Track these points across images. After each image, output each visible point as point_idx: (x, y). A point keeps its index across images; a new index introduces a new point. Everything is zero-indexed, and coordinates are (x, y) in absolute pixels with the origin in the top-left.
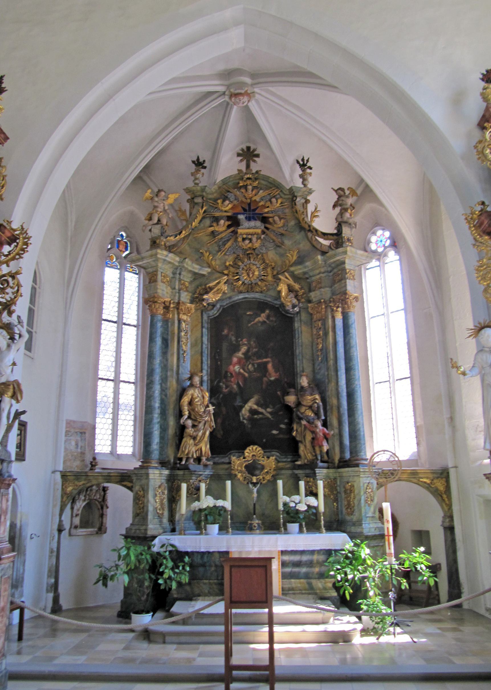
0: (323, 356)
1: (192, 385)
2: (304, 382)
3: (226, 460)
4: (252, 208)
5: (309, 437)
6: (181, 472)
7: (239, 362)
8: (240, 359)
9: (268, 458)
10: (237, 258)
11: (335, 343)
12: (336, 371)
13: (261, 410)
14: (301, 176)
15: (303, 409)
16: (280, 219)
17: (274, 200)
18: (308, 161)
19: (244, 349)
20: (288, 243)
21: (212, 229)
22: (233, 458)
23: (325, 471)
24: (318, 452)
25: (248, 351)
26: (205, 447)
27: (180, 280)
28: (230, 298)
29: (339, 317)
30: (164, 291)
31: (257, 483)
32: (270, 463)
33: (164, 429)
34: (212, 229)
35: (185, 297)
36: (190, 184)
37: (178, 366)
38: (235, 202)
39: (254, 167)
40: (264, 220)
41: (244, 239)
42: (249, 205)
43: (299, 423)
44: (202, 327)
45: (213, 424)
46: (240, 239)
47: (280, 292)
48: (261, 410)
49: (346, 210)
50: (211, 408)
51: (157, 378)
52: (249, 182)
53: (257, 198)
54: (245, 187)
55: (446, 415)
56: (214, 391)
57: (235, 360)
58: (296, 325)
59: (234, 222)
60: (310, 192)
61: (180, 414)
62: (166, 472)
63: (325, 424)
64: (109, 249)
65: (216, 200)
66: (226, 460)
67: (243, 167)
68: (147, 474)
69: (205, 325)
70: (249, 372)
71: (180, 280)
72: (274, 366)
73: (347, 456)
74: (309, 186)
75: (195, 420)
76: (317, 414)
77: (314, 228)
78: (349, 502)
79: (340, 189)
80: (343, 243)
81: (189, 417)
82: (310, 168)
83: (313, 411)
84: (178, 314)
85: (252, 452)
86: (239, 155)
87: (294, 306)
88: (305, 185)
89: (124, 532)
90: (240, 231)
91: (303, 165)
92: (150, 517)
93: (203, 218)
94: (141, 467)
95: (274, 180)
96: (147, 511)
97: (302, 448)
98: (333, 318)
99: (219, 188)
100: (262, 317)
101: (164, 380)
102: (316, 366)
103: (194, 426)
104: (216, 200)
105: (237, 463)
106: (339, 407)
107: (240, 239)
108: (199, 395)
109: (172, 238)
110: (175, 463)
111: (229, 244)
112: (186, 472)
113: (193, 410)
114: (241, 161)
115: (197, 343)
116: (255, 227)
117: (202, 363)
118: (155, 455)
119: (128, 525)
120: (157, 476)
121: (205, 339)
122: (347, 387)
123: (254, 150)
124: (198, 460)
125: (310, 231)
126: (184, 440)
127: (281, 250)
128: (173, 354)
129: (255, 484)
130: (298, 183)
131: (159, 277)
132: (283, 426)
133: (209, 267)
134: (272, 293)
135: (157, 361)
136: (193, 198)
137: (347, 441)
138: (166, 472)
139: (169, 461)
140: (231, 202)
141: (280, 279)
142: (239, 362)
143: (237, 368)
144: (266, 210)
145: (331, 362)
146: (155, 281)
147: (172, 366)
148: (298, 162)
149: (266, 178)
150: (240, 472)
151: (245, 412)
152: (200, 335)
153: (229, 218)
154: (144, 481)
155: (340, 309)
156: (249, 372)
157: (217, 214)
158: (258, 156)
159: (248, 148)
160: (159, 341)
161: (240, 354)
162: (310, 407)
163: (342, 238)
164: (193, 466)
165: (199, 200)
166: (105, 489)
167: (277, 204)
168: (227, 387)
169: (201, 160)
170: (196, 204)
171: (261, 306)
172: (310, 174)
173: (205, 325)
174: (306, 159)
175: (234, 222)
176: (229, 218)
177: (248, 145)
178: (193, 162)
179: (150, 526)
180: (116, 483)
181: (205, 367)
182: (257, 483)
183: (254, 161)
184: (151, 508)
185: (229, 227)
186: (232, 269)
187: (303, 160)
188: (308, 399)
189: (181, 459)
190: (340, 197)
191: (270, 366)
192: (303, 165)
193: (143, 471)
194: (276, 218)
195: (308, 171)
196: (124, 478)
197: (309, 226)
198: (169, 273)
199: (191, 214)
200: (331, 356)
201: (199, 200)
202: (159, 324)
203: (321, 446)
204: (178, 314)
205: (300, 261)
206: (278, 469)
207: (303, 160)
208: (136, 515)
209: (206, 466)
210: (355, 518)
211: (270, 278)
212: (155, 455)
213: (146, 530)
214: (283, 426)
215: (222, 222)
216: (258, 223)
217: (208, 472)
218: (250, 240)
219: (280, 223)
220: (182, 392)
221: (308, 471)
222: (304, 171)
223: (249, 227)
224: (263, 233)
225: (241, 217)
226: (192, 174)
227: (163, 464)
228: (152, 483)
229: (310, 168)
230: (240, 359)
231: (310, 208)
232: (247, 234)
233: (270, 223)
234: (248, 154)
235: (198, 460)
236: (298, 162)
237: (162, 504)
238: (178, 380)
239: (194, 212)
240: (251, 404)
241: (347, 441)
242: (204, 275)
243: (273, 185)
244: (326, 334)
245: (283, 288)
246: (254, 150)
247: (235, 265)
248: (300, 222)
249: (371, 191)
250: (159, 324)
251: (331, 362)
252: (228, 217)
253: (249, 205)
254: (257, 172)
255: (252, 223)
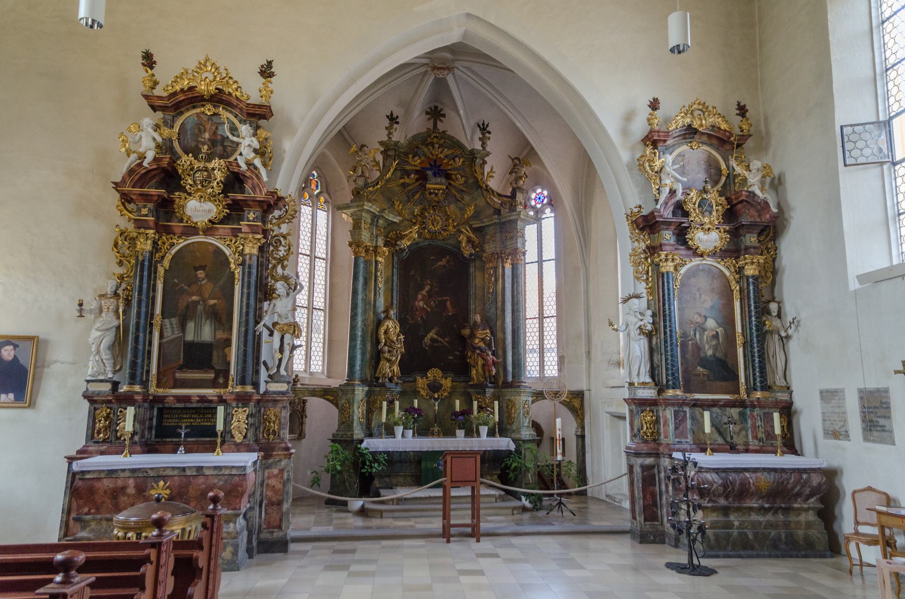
0: (494, 300)
1: (387, 317)
2: (478, 318)
3: (411, 379)
4: (438, 164)
5: (480, 362)
6: (378, 389)
7: (422, 300)
8: (423, 296)
9: (446, 378)
10: (424, 209)
11: (504, 289)
12: (503, 311)
13: (440, 339)
14: (480, 139)
15: (477, 341)
16: (462, 177)
17: (457, 159)
18: (487, 126)
19: (427, 288)
20: (467, 198)
21: (402, 181)
22: (418, 378)
23: (492, 390)
24: (487, 374)
25: (430, 290)
26: (396, 368)
27: (377, 226)
28: (417, 243)
29: (508, 267)
30: (365, 236)
31: (438, 398)
32: (447, 383)
33: (363, 354)
34: (402, 181)
35: (381, 242)
36: (386, 139)
37: (375, 301)
38: (423, 158)
39: (441, 127)
40: (448, 177)
41: (430, 193)
42: (435, 161)
43: (474, 352)
44: (393, 267)
45: (403, 350)
46: (427, 193)
47: (460, 242)
48: (440, 339)
49: (521, 178)
50: (402, 337)
51: (360, 310)
52: (435, 140)
53: (442, 156)
54: (432, 144)
55: (583, 349)
56: (402, 321)
57: (420, 297)
58: (472, 270)
59: (422, 176)
60: (488, 154)
61: (378, 342)
62: (366, 389)
63: (493, 354)
64: (304, 188)
65: (406, 154)
66: (411, 379)
67: (430, 125)
68: (354, 391)
69: (395, 266)
70: (431, 308)
71: (377, 226)
72: (451, 304)
73: (510, 379)
74: (488, 149)
75: (390, 347)
76: (489, 345)
77: (491, 189)
78: (510, 415)
79: (516, 158)
80: (516, 205)
81: (385, 344)
82: (489, 133)
83: (484, 343)
84: (376, 256)
85: (434, 373)
86: (427, 113)
87: (471, 255)
88: (484, 148)
89: (331, 437)
90: (428, 186)
91: (484, 128)
92: (355, 424)
93: (395, 170)
94: (346, 385)
95: (458, 141)
96: (353, 420)
97: (474, 372)
98: (503, 267)
99: (410, 143)
100: (443, 262)
101: (365, 312)
102: (487, 306)
103: (389, 351)
104: (406, 154)
105: (421, 382)
106: (504, 340)
107: (427, 193)
108: (392, 326)
109: (371, 189)
110: (371, 381)
111: (417, 196)
112: (383, 389)
113: (389, 338)
114: (429, 119)
115: (389, 281)
116: (441, 184)
117: (392, 298)
118: (358, 375)
119: (334, 431)
120: (360, 392)
121: (395, 278)
122: (513, 325)
123: (441, 110)
124: (391, 380)
125: (486, 190)
126: (382, 363)
127: (460, 204)
128: (370, 291)
129: (436, 400)
130: (478, 146)
131: (363, 225)
132: (457, 353)
133: (400, 215)
134: (452, 241)
135: (360, 297)
136: (385, 151)
137: (510, 368)
138: (366, 389)
139: (367, 380)
140: (420, 158)
141: (462, 232)
142: (422, 300)
143: (421, 304)
144: (450, 167)
145: (499, 304)
146: (360, 228)
147: (370, 301)
148: (479, 126)
149: (451, 138)
150: (423, 389)
151: (427, 340)
152: (390, 274)
153: (417, 172)
154: (349, 396)
155: (509, 261)
156: (431, 308)
157: (408, 168)
158: (444, 116)
159: (436, 107)
160: (361, 279)
161: (424, 292)
162: (483, 340)
163: (516, 201)
164: (388, 385)
165: (391, 153)
166: (304, 402)
167: (459, 162)
168: (413, 319)
169: (395, 116)
170: (389, 156)
171: (442, 252)
172: (489, 138)
173: (395, 266)
174: (486, 123)
175: (422, 176)
176: (417, 172)
177: (436, 104)
178: (388, 117)
179: (356, 432)
180: (320, 397)
181: (395, 302)
182: (438, 398)
183: (441, 121)
184: (355, 418)
185: (417, 180)
186: (419, 218)
187: (483, 124)
188: (480, 333)
189: (378, 378)
190: (515, 165)
191: (448, 303)
192: (484, 128)
193: (350, 388)
194: (459, 176)
195: (487, 135)
196: (325, 393)
197: (487, 186)
198: (369, 221)
199: (384, 165)
200: (500, 298)
201: (391, 153)
202: (362, 266)
203: (490, 371)
204: (376, 256)
205: (476, 215)
206: (453, 387)
207: (483, 124)
208: (341, 423)
209: (397, 384)
210: (514, 428)
211: (451, 228)
212: (358, 375)
213: (352, 435)
214: (457, 353)
215: (412, 176)
216: (444, 180)
217: (399, 389)
218: (436, 194)
219: (462, 181)
220: (379, 323)
221: (478, 390)
222: (483, 134)
223: (435, 184)
224: (447, 188)
225: (429, 173)
226: (387, 128)
227: (363, 381)
228: (356, 397)
229: (489, 133)
230: (423, 296)
231: (487, 169)
232: (435, 189)
233: (453, 180)
234: (435, 113)
235: (391, 380)
236: (479, 126)
237: (363, 414)
238: (374, 312)
239: (388, 163)
240: (432, 334)
241: (510, 368)
242: (395, 223)
243: (456, 145)
244: (496, 280)
245: (463, 238)
246: (441, 110)
247: (422, 214)
248: (478, 182)
249: (536, 153)
250: (362, 266)
251: (499, 304)
252: (417, 171)
253: (435, 161)
254: (444, 132)
255: (439, 180)
